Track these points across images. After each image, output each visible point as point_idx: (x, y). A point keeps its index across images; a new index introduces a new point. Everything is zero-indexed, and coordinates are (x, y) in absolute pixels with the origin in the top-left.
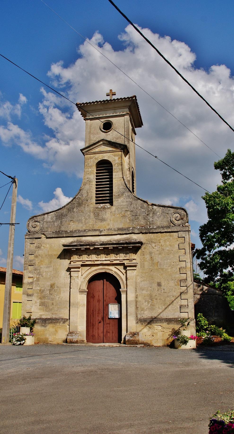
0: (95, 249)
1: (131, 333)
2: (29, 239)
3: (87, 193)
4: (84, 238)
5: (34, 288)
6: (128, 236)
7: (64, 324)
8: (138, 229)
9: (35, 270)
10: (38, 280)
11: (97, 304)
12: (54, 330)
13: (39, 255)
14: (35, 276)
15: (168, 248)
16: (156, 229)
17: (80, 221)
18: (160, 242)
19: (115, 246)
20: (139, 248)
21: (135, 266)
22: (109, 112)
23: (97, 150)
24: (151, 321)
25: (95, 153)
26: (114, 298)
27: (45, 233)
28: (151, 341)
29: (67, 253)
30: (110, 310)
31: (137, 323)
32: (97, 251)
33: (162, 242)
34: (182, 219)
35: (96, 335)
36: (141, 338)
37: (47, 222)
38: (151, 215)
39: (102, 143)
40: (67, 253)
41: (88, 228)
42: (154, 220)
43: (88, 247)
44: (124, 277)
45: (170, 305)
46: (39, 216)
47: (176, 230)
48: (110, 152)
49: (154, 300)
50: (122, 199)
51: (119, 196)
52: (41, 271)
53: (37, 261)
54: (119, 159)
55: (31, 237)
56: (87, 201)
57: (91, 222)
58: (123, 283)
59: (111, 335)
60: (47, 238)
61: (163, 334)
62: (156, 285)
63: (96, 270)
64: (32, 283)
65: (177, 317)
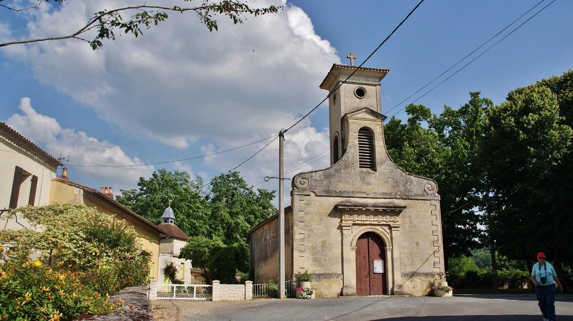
0: (367, 210)
1: (398, 285)
2: (298, 196)
3: (353, 156)
4: (352, 199)
5: (305, 244)
6: (390, 200)
7: (338, 279)
8: (400, 195)
9: (306, 226)
10: (309, 236)
11: (363, 260)
12: (328, 284)
13: (309, 212)
14: (306, 232)
15: (423, 214)
16: (413, 196)
17: (348, 182)
18: (416, 208)
19: (385, 209)
20: (400, 212)
21: (398, 227)
22: (362, 78)
23: (359, 116)
24: (412, 275)
25: (358, 119)
26: (378, 255)
27: (315, 191)
28: (413, 292)
29: (338, 211)
30: (375, 266)
31: (402, 276)
32: (368, 212)
33: (419, 208)
34: (433, 189)
35: (364, 288)
36: (405, 289)
37: (315, 180)
38: (409, 184)
39: (364, 110)
40: (338, 211)
41: (356, 190)
42: (412, 188)
43: (361, 208)
44: (389, 236)
45: (425, 261)
46: (307, 173)
47: (429, 199)
48: (371, 120)
49: (414, 257)
50: (384, 166)
51: (381, 163)
52: (312, 227)
53: (307, 218)
54: (380, 128)
55: (300, 193)
56: (353, 164)
57: (358, 185)
58: (389, 242)
59: (376, 288)
60: (316, 196)
61: (422, 286)
62: (415, 244)
63: (365, 229)
64: (303, 239)
65: (431, 272)
